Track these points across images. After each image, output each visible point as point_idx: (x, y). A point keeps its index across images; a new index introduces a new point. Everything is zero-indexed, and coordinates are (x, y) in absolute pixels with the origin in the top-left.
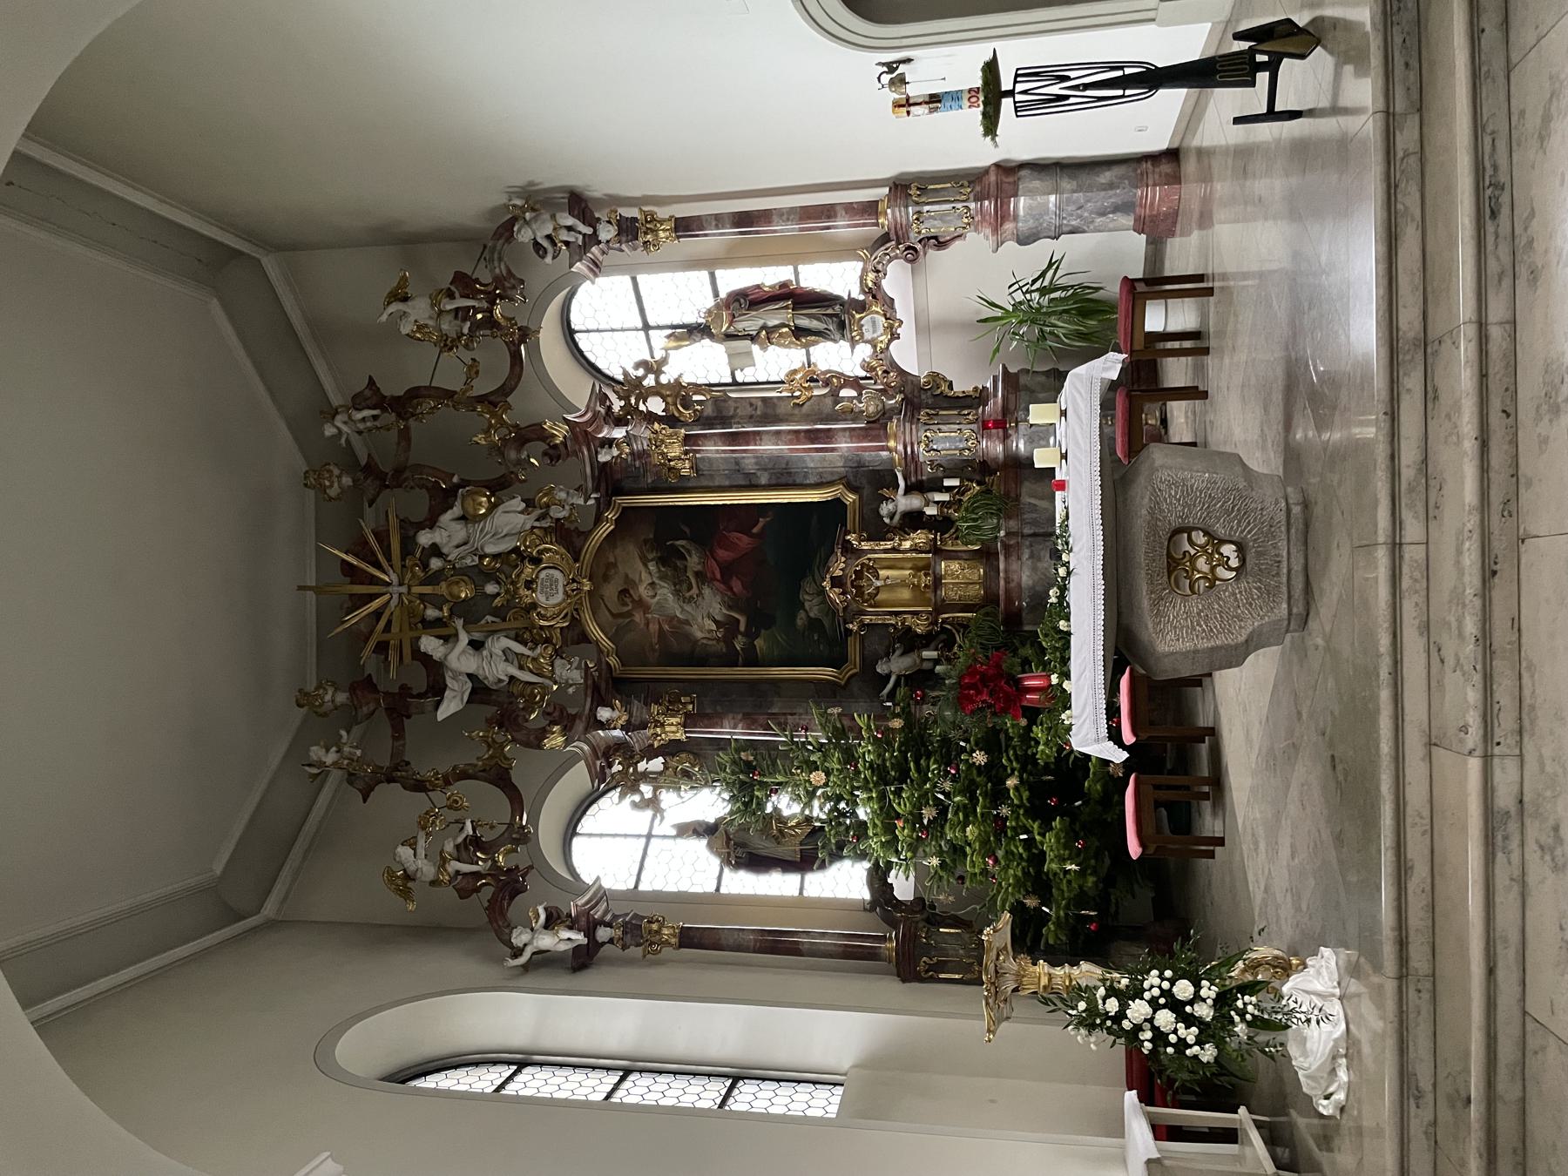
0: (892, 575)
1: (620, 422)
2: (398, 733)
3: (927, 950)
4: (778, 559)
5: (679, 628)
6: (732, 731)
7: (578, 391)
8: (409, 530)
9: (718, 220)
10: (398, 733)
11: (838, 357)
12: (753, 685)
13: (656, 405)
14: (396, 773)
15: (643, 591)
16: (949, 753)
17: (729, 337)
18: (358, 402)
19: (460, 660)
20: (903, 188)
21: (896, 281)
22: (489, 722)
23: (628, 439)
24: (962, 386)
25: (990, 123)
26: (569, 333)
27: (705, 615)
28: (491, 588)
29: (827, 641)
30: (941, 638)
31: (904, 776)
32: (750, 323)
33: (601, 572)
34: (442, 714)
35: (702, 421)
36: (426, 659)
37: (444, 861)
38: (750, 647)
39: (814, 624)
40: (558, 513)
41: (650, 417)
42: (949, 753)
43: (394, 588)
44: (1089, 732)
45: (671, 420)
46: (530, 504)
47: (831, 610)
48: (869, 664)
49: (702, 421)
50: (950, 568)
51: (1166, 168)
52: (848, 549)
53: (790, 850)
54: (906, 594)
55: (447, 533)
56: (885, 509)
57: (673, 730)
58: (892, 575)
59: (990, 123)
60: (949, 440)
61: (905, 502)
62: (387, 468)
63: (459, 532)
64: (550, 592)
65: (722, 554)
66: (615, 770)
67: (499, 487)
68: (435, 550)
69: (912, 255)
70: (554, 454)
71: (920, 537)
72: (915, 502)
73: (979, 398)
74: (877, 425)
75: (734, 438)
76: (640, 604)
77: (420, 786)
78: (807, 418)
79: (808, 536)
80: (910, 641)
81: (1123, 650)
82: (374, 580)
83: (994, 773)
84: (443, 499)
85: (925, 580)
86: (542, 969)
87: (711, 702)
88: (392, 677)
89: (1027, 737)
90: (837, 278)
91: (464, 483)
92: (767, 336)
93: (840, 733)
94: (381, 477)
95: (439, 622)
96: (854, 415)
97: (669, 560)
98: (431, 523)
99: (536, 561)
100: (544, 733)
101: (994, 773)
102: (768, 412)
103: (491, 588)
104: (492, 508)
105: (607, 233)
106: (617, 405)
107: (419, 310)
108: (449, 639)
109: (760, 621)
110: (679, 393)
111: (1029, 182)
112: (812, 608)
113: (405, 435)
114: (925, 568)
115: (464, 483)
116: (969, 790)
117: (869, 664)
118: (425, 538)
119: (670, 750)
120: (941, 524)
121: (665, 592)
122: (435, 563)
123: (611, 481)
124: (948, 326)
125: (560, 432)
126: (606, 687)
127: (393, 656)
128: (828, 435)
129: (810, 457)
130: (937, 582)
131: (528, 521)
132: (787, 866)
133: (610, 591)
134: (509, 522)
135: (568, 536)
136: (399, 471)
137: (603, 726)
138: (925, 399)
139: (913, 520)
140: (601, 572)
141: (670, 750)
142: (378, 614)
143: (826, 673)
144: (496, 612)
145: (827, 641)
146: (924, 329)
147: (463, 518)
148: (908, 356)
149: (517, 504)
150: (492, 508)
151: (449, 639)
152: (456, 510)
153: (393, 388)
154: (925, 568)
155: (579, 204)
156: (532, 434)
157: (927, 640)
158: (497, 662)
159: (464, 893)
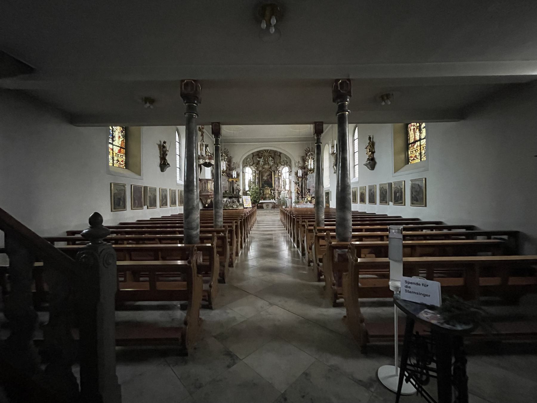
0: (268, 191)
4: (269, 183)
7: (280, 169)
8: (271, 156)
14: (253, 156)
19: (261, 160)
20: (291, 192)
21: (286, 192)
27: (265, 178)
29: (263, 187)
30: (264, 194)
43: (266, 154)
44: (261, 201)
55: (271, 159)
57: (257, 176)
58: (268, 191)
61: (273, 192)
64: (266, 166)
70: (276, 167)
74: (278, 190)
79: (270, 185)
81: (264, 203)
84: (273, 158)
86: (243, 170)
87: (259, 178)
88: (260, 155)
90: (287, 188)
97: (269, 175)
102: (279, 182)
110: (280, 176)
121: (266, 175)
123: (274, 171)
126: (260, 172)
134: (272, 164)
135: (270, 168)
138: (279, 193)
145: (263, 187)
158: (261, 163)
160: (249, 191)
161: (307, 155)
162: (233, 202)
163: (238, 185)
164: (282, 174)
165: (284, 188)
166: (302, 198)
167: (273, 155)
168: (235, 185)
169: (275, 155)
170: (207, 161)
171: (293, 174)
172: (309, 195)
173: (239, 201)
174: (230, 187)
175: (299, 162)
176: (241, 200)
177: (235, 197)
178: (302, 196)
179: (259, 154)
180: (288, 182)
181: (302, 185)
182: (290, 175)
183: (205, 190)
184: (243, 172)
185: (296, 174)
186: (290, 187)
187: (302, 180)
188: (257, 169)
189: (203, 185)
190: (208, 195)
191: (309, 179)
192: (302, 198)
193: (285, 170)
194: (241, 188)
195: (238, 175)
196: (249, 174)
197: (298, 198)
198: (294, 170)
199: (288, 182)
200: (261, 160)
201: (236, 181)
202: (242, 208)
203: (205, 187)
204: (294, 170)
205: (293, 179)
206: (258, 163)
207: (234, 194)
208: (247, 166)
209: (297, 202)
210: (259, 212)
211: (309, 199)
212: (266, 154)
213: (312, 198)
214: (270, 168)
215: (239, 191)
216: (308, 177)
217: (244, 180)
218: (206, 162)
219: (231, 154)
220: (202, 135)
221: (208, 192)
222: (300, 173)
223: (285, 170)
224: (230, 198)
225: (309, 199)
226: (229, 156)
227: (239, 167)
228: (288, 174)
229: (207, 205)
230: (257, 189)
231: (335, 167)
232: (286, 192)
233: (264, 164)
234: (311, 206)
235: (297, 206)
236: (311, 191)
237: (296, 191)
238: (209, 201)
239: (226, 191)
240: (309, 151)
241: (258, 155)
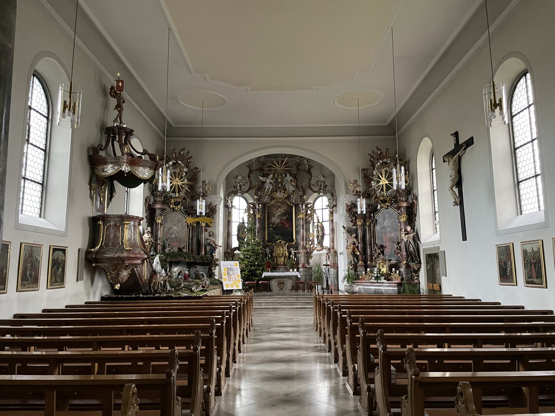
0: (282, 250)
1: (306, 206)
2: (257, 170)
3: (229, 256)
5: (274, 216)
6: (257, 225)
7: (310, 201)
8: (289, 172)
9: (333, 226)
10: (257, 170)
11: (316, 242)
12: (265, 227)
13: (309, 212)
14: (251, 171)
15: (279, 210)
16: (257, 259)
17: (318, 226)
18: (309, 166)
19: (268, 181)
20: (336, 252)
22: (258, 186)
23: (303, 209)
24: (310, 261)
25: (324, 265)
26: (322, 196)
27: (276, 220)
28: (280, 185)
29: (272, 239)
31: (253, 253)
32: (319, 229)
33: (282, 203)
34: (260, 177)
35: (306, 219)
36: (268, 175)
37: (239, 183)
38: (270, 227)
39: (274, 237)
40: (292, 196)
41: (307, 211)
42: (257, 259)
43: (279, 168)
44: (265, 274)
45: (307, 214)
46: (293, 191)
47: (276, 241)
48: (268, 246)
49: (306, 219)
50: (283, 259)
51: (336, 289)
52: (286, 243)
53: (240, 235)
54: (279, 252)
55: (289, 178)
56: (292, 249)
57: (258, 216)
58: (282, 250)
59: (324, 265)
60: (302, 259)
61: (293, 252)
62: (300, 167)
63: (289, 180)
64: (279, 195)
65: (285, 223)
66: (251, 207)
67: (297, 186)
68: (286, 176)
69: (327, 254)
70: (301, 197)
71: (287, 254)
72: (293, 253)
73: (308, 264)
74: (304, 248)
75: (303, 226)
76: (277, 209)
77: (249, 177)
78: (306, 237)
79: (288, 237)
80: (271, 253)
82: (281, 164)
83: (254, 265)
84: (295, 177)
85: (281, 255)
86: (226, 201)
87: (262, 221)
89: (259, 270)
90: (327, 242)
91: (297, 180)
92: (318, 232)
93: (258, 243)
94: (298, 166)
95: (274, 176)
96: (306, 244)
97: (284, 214)
98: (291, 175)
99: (284, 192)
100: (257, 196)
101: (254, 265)
102: (308, 230)
103: (280, 185)
104: (293, 185)
105: (331, 210)
106: (309, 206)
107: (322, 179)
108: (272, 179)
109: (275, 229)
110: (311, 216)
111: (335, 271)
112: (277, 237)
113: (304, 171)
114: (283, 255)
115: (297, 180)
116: (252, 262)
117: (268, 246)
118: (288, 175)
119: (254, 215)
120: (289, 257)
121: (279, 213)
122: (284, 176)
123: (297, 206)
124: (320, 258)
125: (305, 197)
126: (264, 205)
127: (269, 169)
128: (303, 240)
129: (300, 237)
130: (280, 257)
131: (291, 192)
132: (238, 235)
133: (279, 204)
134: (291, 189)
135: (288, 197)
136: (299, 169)
137: (259, 206)
138: (308, 255)
139: (290, 253)
140: (282, 203)
141: (254, 215)
142: (276, 165)
143: (266, 239)
144: (276, 185)
145: (272, 239)
146: (320, 255)
147: (291, 180)
148: (315, 252)
149: (293, 189)
150: (293, 185)
151: (272, 179)
152: (293, 179)
153: (312, 171)
154: (283, 255)
155: (335, 206)
156: (304, 194)
157: (272, 255)
158: (268, 186)
159: (234, 186)
160: (238, 248)
161: (373, 166)
162: (197, 277)
163: (212, 235)
164: (314, 211)
165: (320, 243)
166: (366, 267)
167: (294, 170)
168: (204, 235)
169: (298, 170)
170: (125, 168)
171: (342, 210)
172: (384, 261)
173: (211, 275)
174: (190, 239)
175: (356, 181)
176: (216, 271)
177: (202, 264)
178: (365, 262)
179: (262, 166)
180: (327, 231)
181: (364, 236)
182: (332, 213)
183: (114, 245)
184: (226, 206)
185: (351, 208)
186: (332, 241)
187: (363, 225)
188: (259, 200)
189: (112, 231)
190: (122, 260)
191: (380, 220)
192: (366, 267)
193: (321, 204)
194: (220, 241)
195: (211, 211)
196: (240, 209)
197: (355, 267)
198: (344, 200)
199: (327, 231)
200: (268, 181)
201: (207, 226)
202: (215, 292)
203: (116, 237)
204: (344, 200)
205: (342, 219)
206: (261, 187)
207: (198, 257)
208: (235, 193)
209: (353, 278)
210: (260, 301)
211: (384, 270)
212: (279, 168)
213: (391, 267)
214: (288, 197)
215: (213, 249)
216: (379, 217)
217: (228, 223)
218: (121, 173)
219: (196, 163)
220: (119, 107)
221: (123, 250)
222: (362, 205)
223: (321, 204)
224: (190, 265)
225: (384, 270)
226: (192, 166)
227: (215, 192)
228: (327, 212)
229: (117, 287)
230: (258, 244)
231: (456, 190)
232: (325, 251)
233: (275, 190)
234: (388, 288)
235: (356, 288)
236: (386, 251)
237: (350, 250)
238: (125, 274)
239: (180, 250)
240: (380, 156)
241: (261, 169)
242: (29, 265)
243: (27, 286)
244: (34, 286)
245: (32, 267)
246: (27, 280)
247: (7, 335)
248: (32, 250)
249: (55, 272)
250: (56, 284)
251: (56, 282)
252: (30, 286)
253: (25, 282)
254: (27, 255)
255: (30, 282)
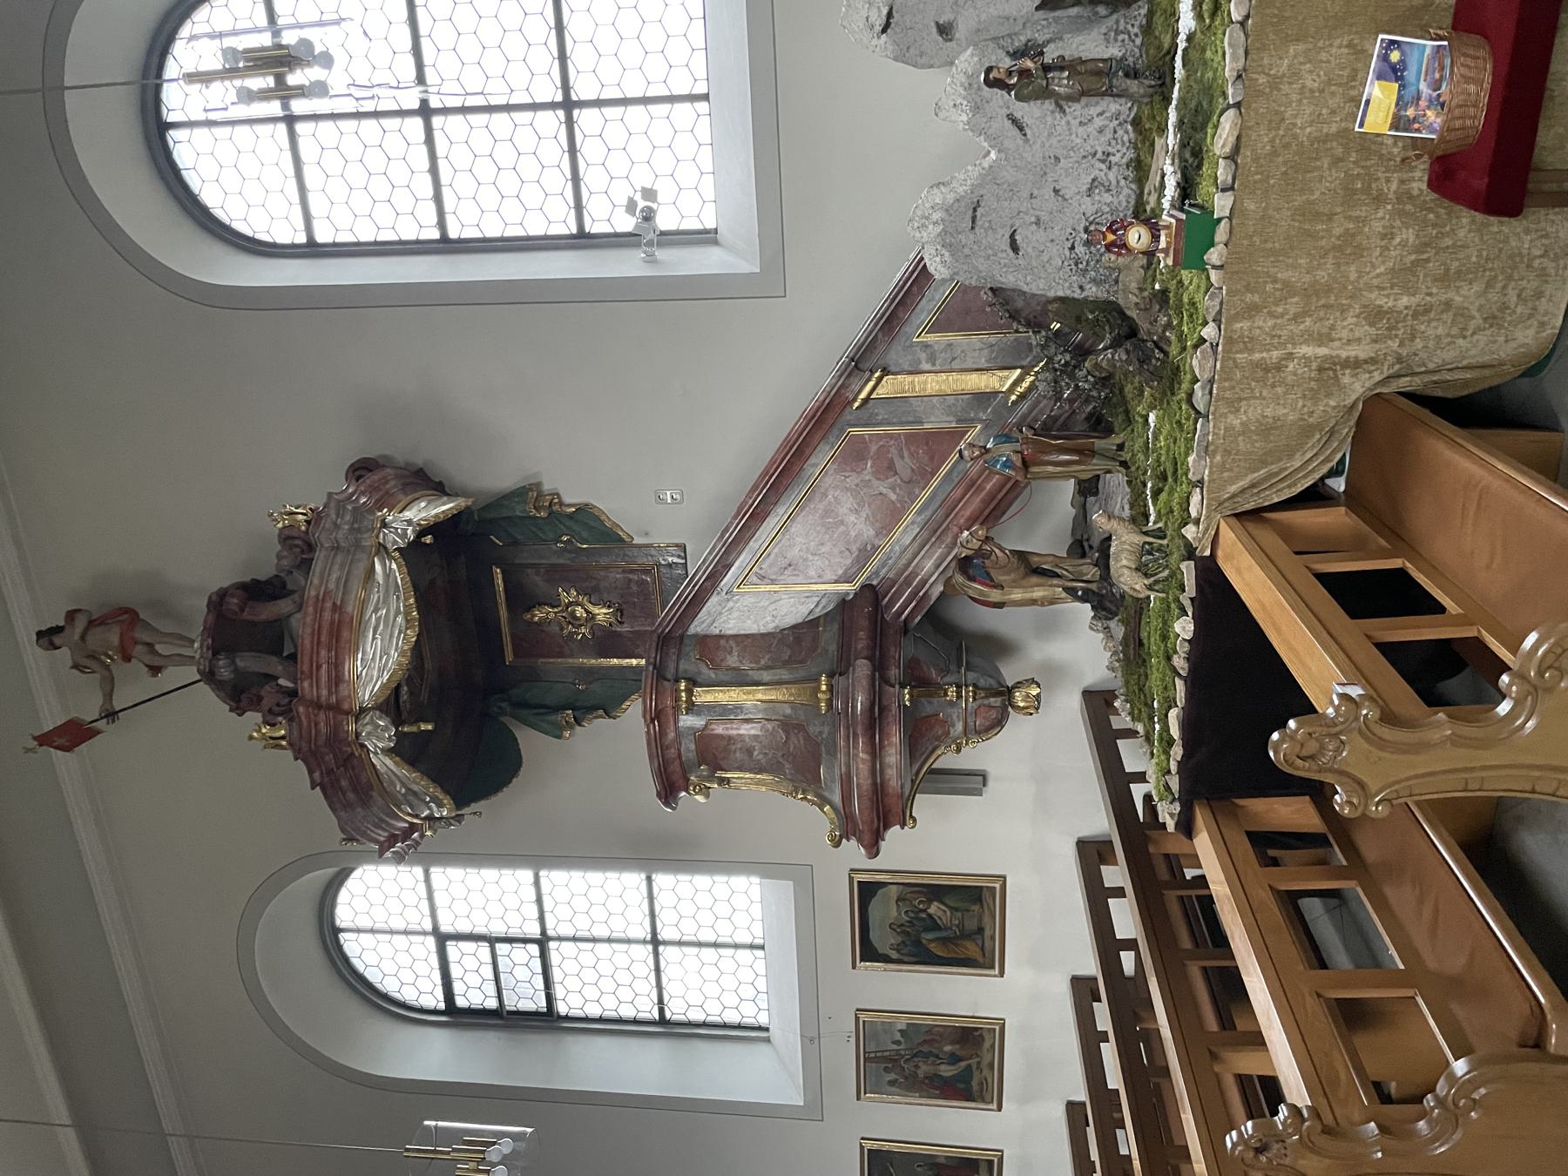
242: (924, 1069)
243: (986, 1072)
244: (987, 1044)
245: (927, 1055)
246: (967, 1074)
247: (1123, 1151)
248: (876, 1060)
249: (944, 941)
250: (987, 933)
251: (981, 930)
252: (986, 1059)
253: (974, 1083)
254: (892, 1076)
255: (973, 1062)
